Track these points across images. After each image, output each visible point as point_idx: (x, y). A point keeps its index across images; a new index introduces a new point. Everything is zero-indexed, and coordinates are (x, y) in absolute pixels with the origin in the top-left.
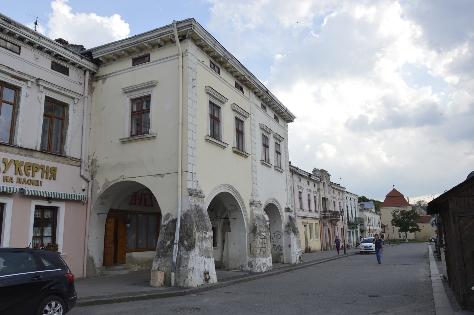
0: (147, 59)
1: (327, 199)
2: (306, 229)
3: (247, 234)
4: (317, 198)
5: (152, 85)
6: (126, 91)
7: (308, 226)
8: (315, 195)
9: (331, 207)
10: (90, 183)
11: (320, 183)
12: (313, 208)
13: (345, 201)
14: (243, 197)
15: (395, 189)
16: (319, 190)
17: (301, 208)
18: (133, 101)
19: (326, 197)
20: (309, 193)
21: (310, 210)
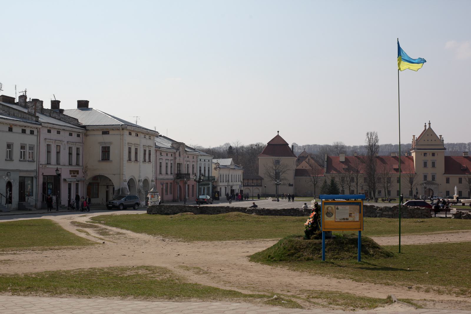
0: (108, 133)
1: (182, 163)
2: (163, 187)
3: (137, 192)
4: (173, 164)
5: (111, 143)
6: (100, 143)
7: (164, 185)
8: (172, 162)
9: (184, 171)
10: (85, 174)
11: (176, 153)
12: (169, 172)
13: (199, 162)
14: (136, 179)
15: (279, 135)
16: (175, 158)
17: (160, 173)
18: (102, 147)
19: (180, 163)
20: (167, 162)
21: (167, 174)
